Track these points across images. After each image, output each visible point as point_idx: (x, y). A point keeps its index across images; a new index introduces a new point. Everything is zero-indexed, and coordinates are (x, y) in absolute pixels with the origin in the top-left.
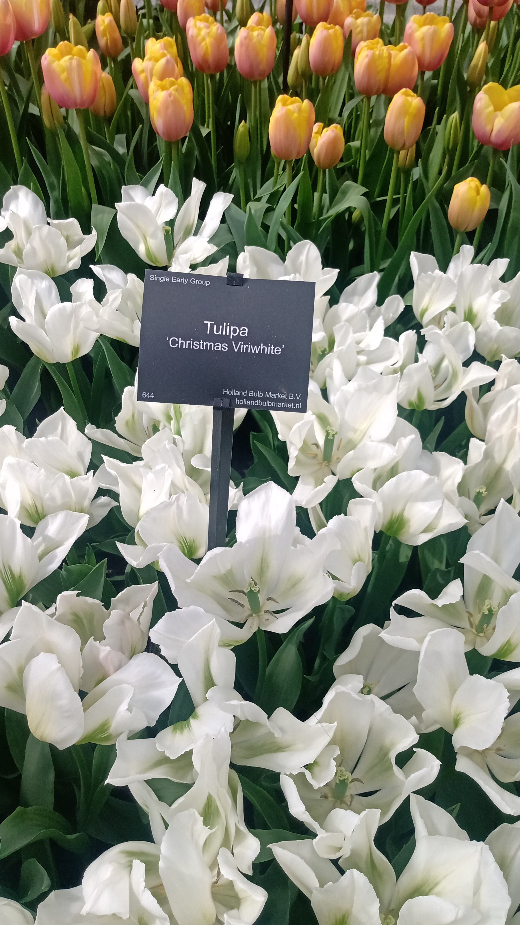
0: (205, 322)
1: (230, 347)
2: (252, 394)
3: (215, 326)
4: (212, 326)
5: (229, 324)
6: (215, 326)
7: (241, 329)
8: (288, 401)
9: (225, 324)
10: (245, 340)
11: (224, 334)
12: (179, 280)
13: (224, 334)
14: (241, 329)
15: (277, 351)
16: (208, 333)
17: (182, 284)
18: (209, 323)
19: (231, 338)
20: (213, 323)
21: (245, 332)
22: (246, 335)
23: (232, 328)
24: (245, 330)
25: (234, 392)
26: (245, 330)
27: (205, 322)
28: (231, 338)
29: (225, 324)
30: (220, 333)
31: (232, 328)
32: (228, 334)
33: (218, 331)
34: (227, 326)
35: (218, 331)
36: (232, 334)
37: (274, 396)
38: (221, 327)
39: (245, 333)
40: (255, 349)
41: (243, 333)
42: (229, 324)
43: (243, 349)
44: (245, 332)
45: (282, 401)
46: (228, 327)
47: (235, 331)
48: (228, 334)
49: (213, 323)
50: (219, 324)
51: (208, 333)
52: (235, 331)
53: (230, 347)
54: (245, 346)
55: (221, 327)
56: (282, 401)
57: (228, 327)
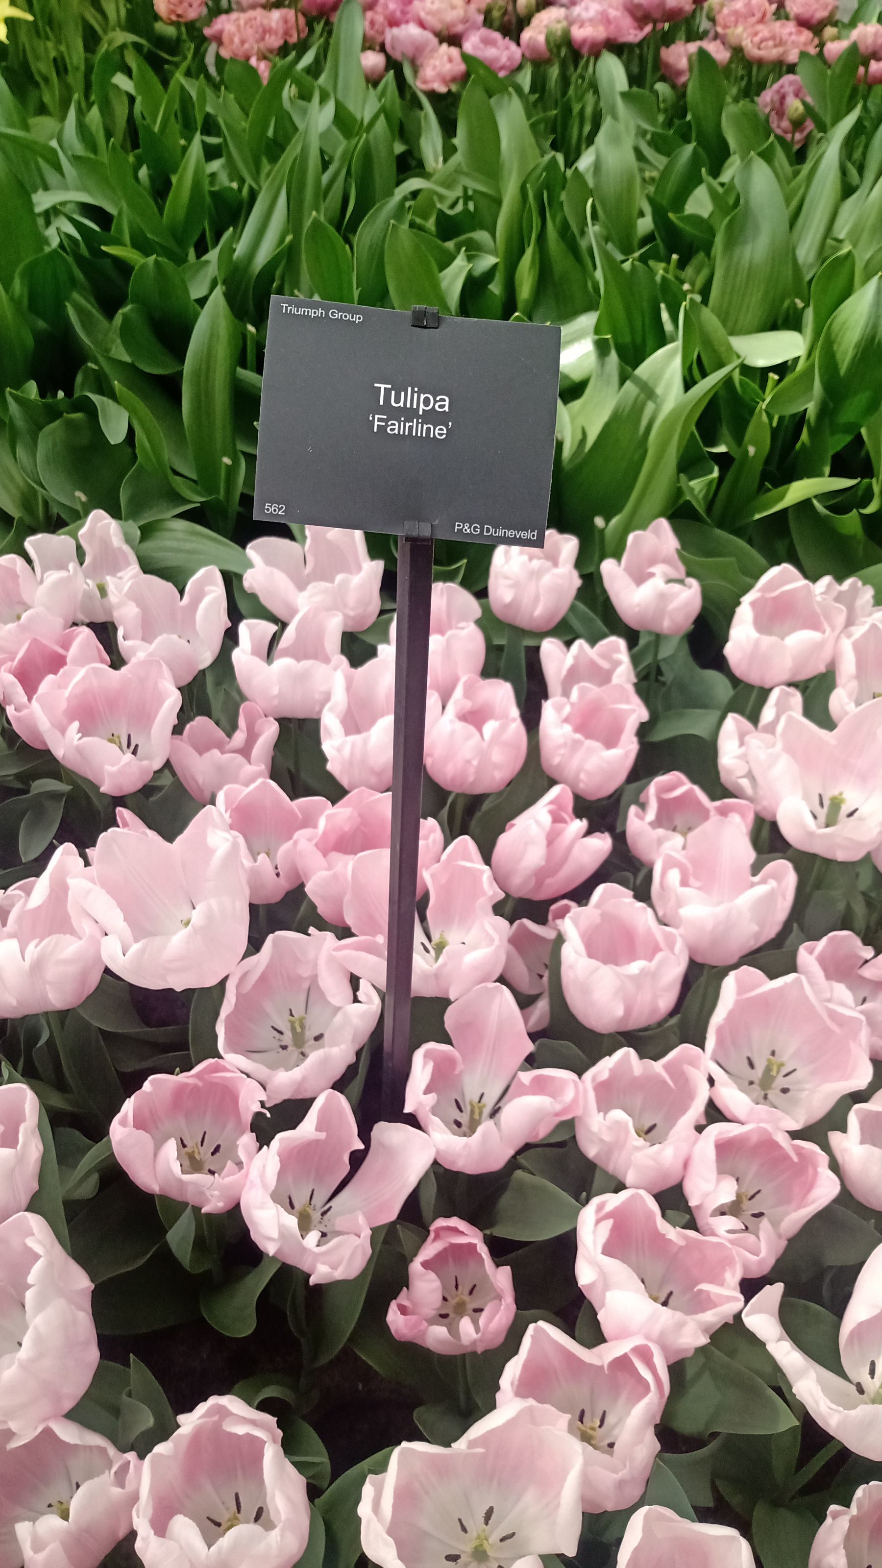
0: (376, 385)
3: (393, 392)
4: (387, 392)
5: (416, 389)
6: (393, 392)
7: (438, 399)
9: (410, 389)
11: (408, 406)
13: (408, 406)
14: (438, 399)
16: (381, 403)
18: (383, 386)
19: (421, 413)
20: (390, 386)
21: (444, 404)
22: (446, 409)
23: (422, 397)
24: (445, 400)
26: (445, 400)
27: (376, 385)
28: (421, 413)
29: (410, 389)
30: (402, 404)
31: (422, 397)
32: (415, 407)
33: (397, 401)
34: (413, 392)
35: (397, 401)
36: (422, 406)
38: (403, 394)
39: (444, 406)
41: (440, 407)
42: (416, 389)
44: (444, 404)
46: (416, 395)
47: (427, 402)
48: (415, 407)
49: (390, 386)
51: (381, 403)
52: (427, 402)
54: (425, 427)
55: (403, 394)
57: (416, 395)
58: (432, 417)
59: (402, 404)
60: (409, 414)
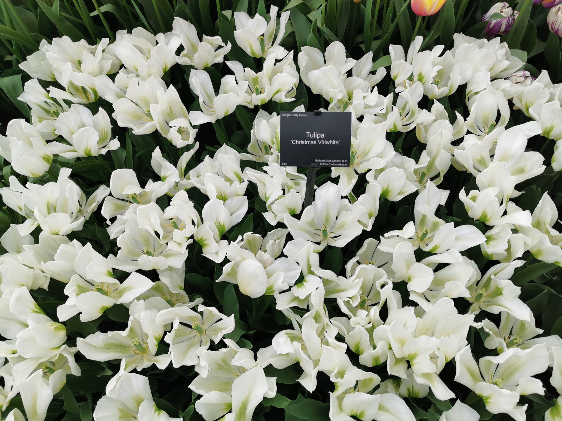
1: (317, 142)
2: (327, 161)
8: (342, 163)
10: (323, 139)
12: (295, 115)
15: (337, 143)
17: (296, 117)
18: (308, 133)
21: (323, 136)
25: (319, 161)
37: (336, 161)
40: (328, 143)
43: (323, 143)
44: (323, 136)
45: (339, 163)
50: (312, 133)
53: (317, 142)
56: (339, 163)
58: (320, 139)
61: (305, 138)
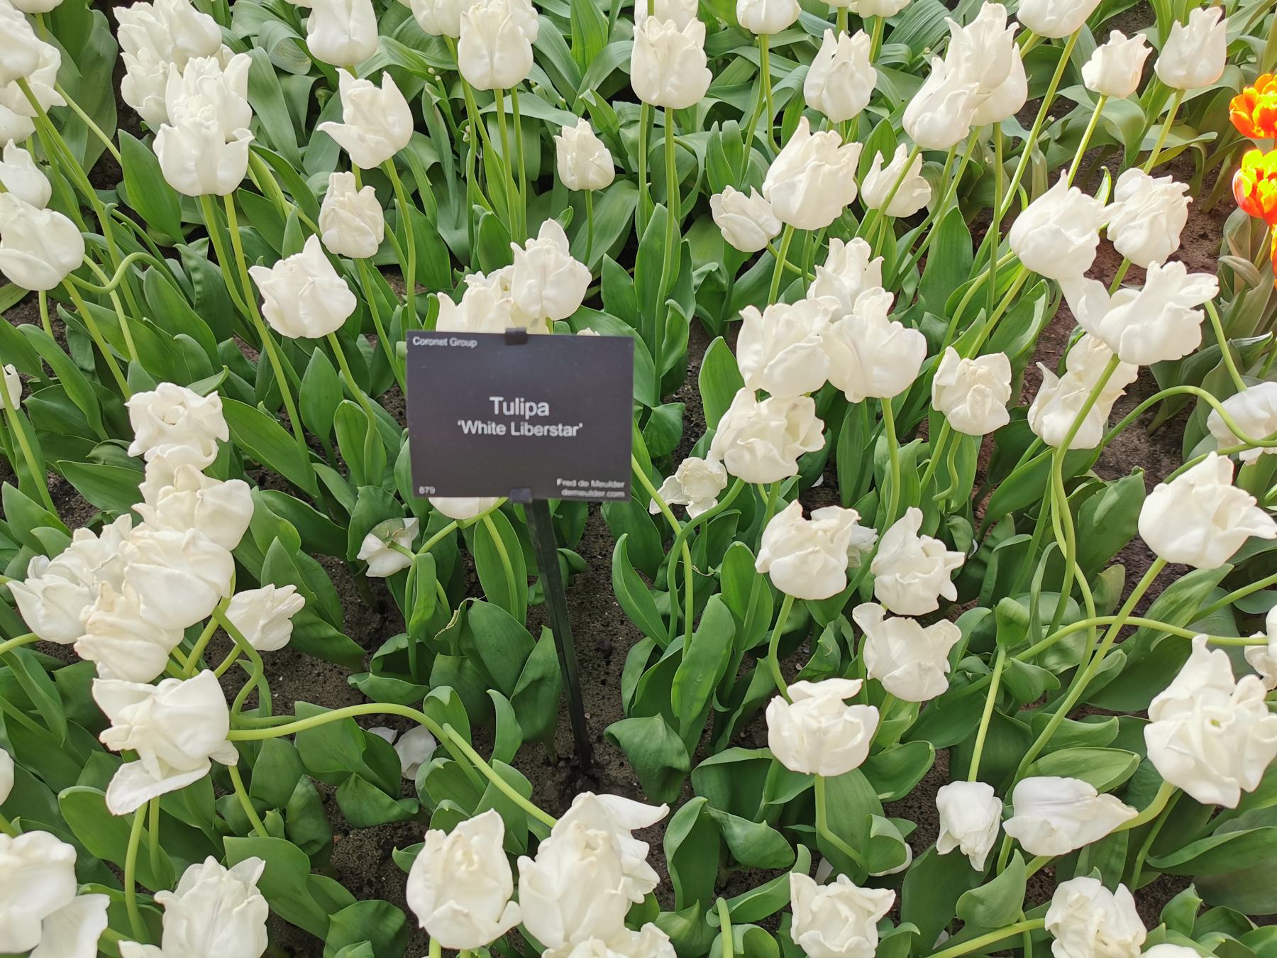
0: (492, 399)
3: (505, 404)
4: (501, 403)
6: (505, 404)
16: (497, 412)
18: (496, 399)
20: (501, 399)
22: (547, 413)
27: (492, 399)
33: (509, 409)
35: (509, 409)
44: (544, 409)
45: (599, 489)
47: (531, 409)
50: (509, 399)
51: (497, 412)
52: (531, 409)
59: (512, 412)
60: (519, 419)
61: (487, 415)
